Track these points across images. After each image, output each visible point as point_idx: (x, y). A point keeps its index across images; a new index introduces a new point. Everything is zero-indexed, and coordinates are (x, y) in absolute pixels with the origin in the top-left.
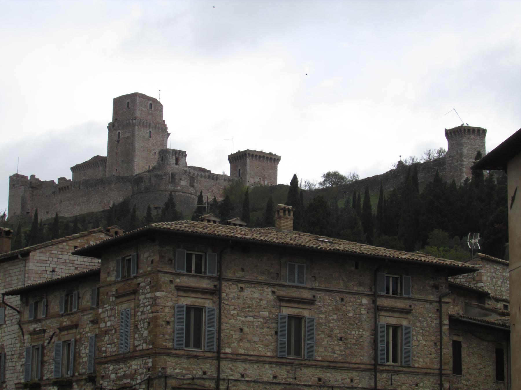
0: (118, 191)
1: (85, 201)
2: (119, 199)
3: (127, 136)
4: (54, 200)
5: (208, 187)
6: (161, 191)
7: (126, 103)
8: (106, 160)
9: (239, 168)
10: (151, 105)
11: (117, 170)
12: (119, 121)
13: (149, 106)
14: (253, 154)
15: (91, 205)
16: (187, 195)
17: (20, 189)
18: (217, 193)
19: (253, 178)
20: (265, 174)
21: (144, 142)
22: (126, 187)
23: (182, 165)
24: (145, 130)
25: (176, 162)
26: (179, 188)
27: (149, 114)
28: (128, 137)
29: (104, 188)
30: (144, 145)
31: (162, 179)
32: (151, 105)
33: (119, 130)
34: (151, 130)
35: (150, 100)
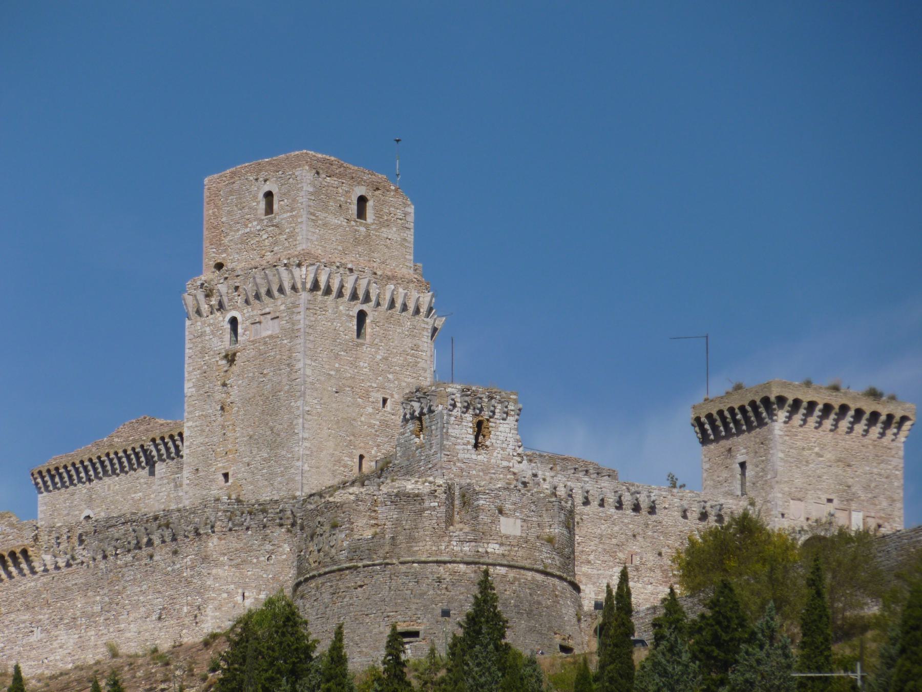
0: (237, 566)
1: (97, 608)
2: (239, 598)
3: (269, 333)
5: (614, 541)
6: (419, 562)
7: (261, 195)
8: (181, 435)
9: (741, 458)
10: (362, 200)
11: (226, 476)
12: (233, 270)
13: (354, 207)
14: (800, 397)
16: (530, 574)
18: (650, 565)
19: (799, 500)
20: (850, 482)
21: (337, 356)
22: (268, 547)
23: (503, 449)
24: (341, 308)
25: (477, 438)
26: (493, 548)
27: (357, 242)
28: (271, 337)
29: (175, 553)
30: (338, 370)
31: (424, 510)
32: (362, 200)
34: (365, 307)
35: (359, 184)
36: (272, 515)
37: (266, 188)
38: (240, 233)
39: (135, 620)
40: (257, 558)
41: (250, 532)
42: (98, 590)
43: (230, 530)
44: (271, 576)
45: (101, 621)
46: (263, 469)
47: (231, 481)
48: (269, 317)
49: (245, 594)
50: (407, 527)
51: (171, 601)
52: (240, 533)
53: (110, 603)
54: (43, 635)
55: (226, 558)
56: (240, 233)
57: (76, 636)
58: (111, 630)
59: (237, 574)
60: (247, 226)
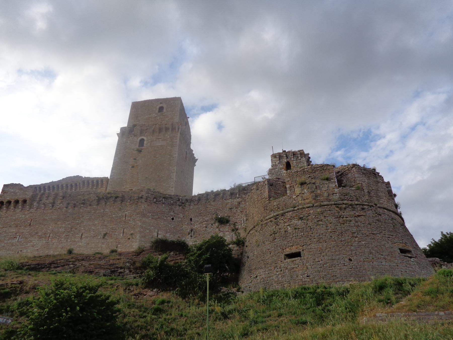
0: (156, 219)
2: (155, 234)
3: (160, 144)
7: (158, 107)
15: (77, 240)
22: (172, 213)
33: (144, 136)
36: (175, 201)
37: (161, 105)
38: (147, 117)
39: (87, 237)
42: (65, 222)
43: (155, 203)
44: (173, 226)
45: (63, 236)
48: (161, 140)
49: (159, 233)
51: (113, 231)
52: (159, 205)
53: (71, 228)
54: (22, 239)
55: (150, 214)
56: (147, 117)
57: (45, 242)
58: (69, 241)
59: (156, 223)
60: (150, 115)
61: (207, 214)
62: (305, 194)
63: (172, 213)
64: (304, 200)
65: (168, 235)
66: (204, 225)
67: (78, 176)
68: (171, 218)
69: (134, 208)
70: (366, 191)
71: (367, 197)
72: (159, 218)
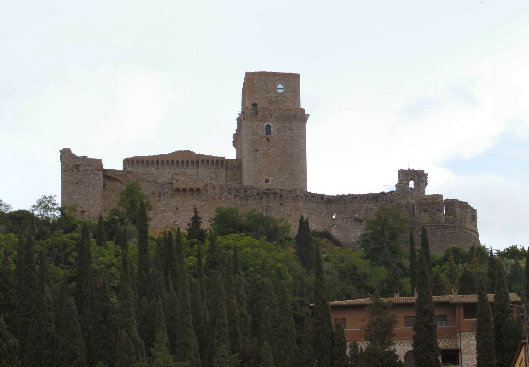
0: (309, 214)
4: (160, 204)
17: (94, 174)
22: (319, 210)
38: (266, 95)
40: (316, 213)
41: (313, 203)
46: (287, 181)
47: (270, 183)
49: (313, 225)
50: (464, 216)
56: (266, 95)
60: (269, 94)
61: (347, 213)
62: (427, 218)
63: (319, 210)
64: (426, 221)
65: (318, 227)
66: (345, 222)
67: (188, 152)
68: (319, 213)
69: (293, 205)
70: (459, 218)
71: (459, 222)
72: (311, 213)
